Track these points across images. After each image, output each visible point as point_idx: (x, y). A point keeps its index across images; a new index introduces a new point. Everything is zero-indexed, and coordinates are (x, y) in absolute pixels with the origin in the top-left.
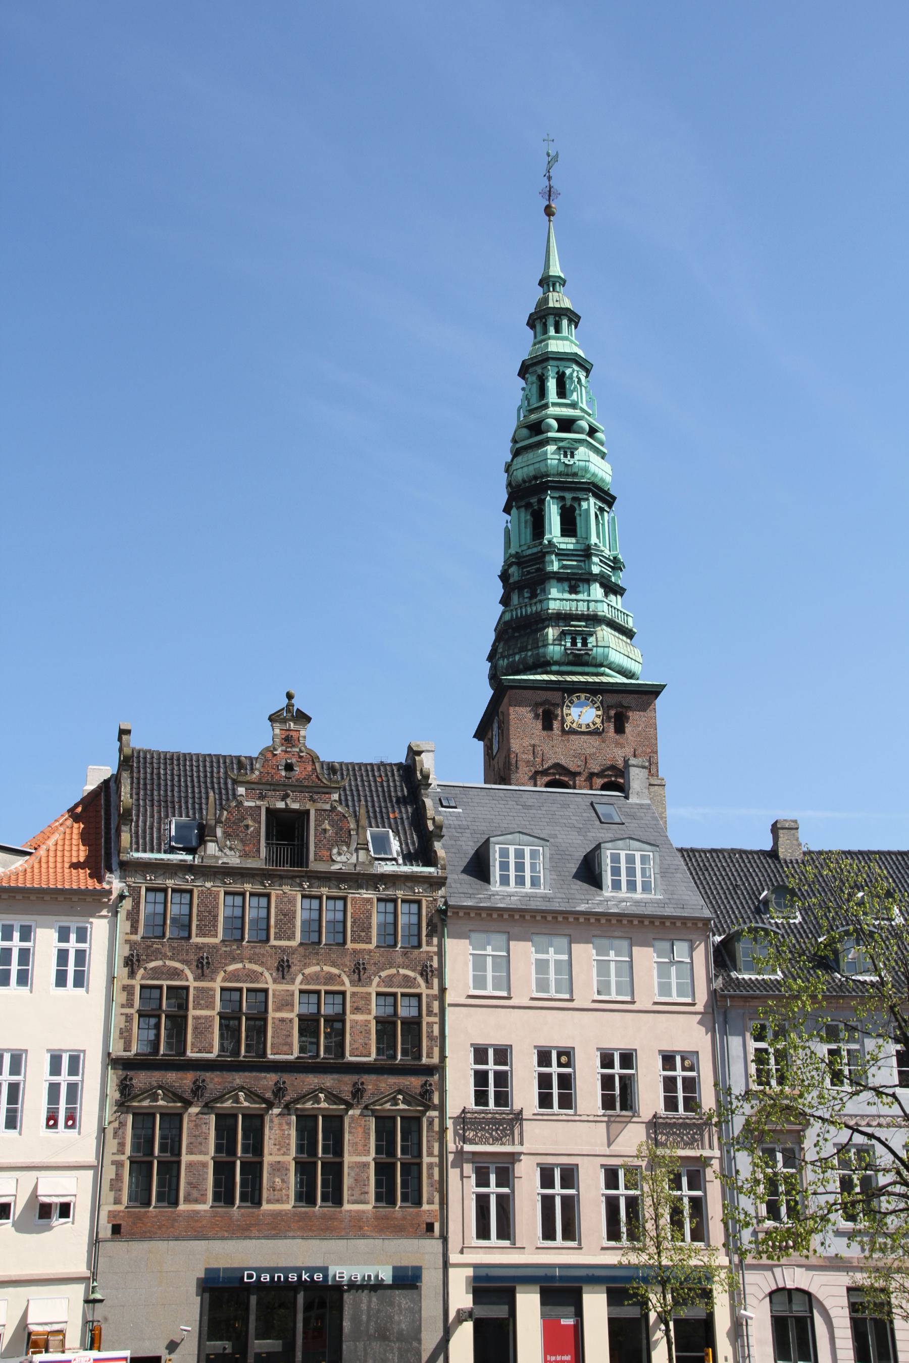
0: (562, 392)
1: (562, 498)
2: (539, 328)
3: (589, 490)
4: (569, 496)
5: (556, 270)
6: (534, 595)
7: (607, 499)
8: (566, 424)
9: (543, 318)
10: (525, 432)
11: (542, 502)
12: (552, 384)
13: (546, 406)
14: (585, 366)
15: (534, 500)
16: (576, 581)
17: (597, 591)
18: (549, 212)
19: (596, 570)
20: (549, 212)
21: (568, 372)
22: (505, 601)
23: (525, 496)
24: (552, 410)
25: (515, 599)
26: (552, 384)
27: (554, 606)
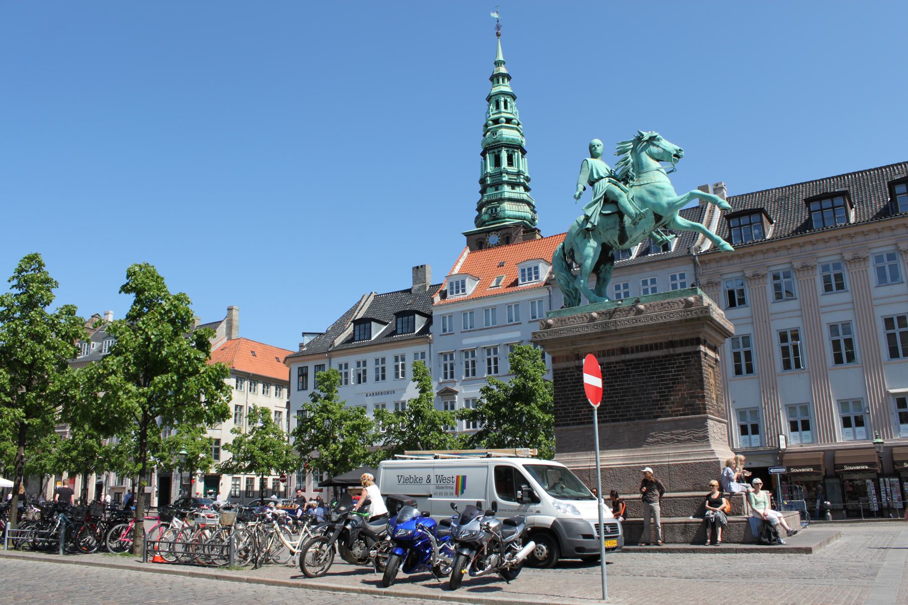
0: (506, 107)
1: (507, 151)
2: (495, 79)
3: (518, 149)
4: (511, 150)
5: (501, 58)
6: (497, 189)
7: (524, 152)
8: (509, 121)
9: (495, 78)
10: (491, 122)
11: (500, 151)
12: (502, 104)
13: (500, 112)
14: (514, 97)
15: (496, 151)
16: (513, 185)
17: (522, 189)
18: (498, 35)
19: (522, 181)
20: (498, 35)
21: (508, 100)
22: (483, 192)
23: (492, 149)
24: (503, 115)
25: (489, 189)
26: (502, 104)
27: (507, 195)
